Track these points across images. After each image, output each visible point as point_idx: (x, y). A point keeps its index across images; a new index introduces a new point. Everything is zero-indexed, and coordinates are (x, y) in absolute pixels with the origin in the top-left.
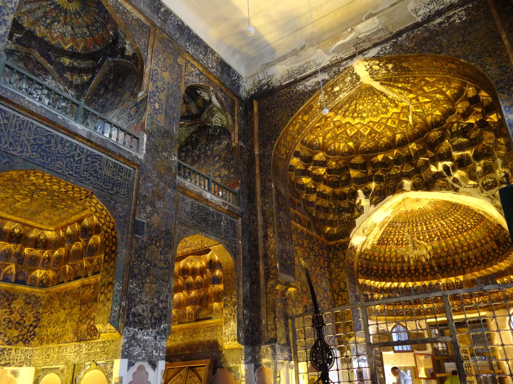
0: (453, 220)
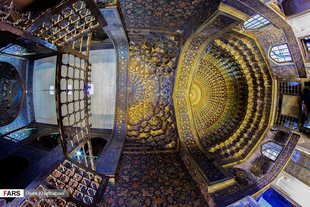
0: (214, 80)
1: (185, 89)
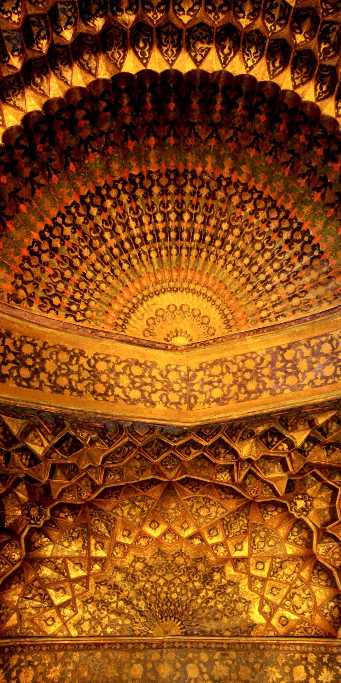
0: (107, 235)
1: (155, 372)
